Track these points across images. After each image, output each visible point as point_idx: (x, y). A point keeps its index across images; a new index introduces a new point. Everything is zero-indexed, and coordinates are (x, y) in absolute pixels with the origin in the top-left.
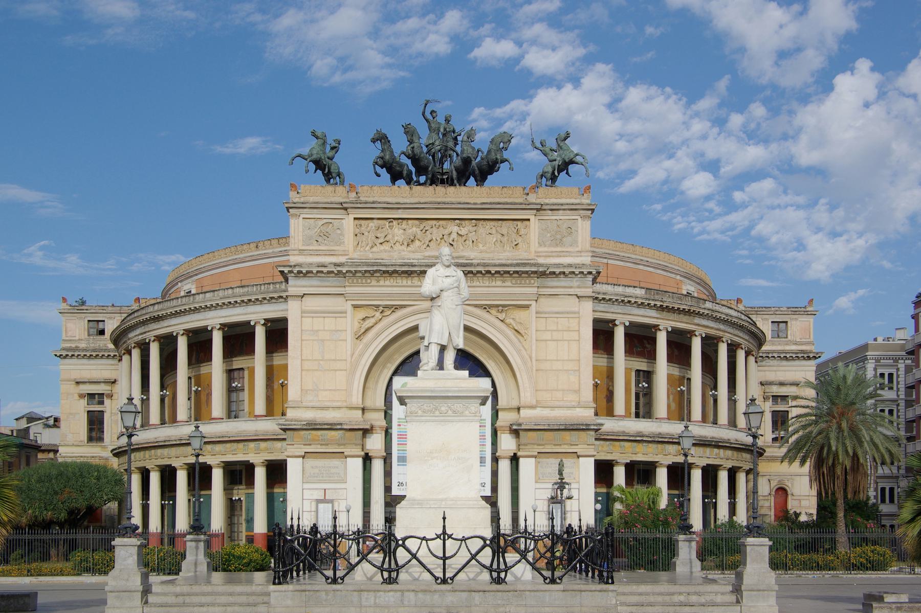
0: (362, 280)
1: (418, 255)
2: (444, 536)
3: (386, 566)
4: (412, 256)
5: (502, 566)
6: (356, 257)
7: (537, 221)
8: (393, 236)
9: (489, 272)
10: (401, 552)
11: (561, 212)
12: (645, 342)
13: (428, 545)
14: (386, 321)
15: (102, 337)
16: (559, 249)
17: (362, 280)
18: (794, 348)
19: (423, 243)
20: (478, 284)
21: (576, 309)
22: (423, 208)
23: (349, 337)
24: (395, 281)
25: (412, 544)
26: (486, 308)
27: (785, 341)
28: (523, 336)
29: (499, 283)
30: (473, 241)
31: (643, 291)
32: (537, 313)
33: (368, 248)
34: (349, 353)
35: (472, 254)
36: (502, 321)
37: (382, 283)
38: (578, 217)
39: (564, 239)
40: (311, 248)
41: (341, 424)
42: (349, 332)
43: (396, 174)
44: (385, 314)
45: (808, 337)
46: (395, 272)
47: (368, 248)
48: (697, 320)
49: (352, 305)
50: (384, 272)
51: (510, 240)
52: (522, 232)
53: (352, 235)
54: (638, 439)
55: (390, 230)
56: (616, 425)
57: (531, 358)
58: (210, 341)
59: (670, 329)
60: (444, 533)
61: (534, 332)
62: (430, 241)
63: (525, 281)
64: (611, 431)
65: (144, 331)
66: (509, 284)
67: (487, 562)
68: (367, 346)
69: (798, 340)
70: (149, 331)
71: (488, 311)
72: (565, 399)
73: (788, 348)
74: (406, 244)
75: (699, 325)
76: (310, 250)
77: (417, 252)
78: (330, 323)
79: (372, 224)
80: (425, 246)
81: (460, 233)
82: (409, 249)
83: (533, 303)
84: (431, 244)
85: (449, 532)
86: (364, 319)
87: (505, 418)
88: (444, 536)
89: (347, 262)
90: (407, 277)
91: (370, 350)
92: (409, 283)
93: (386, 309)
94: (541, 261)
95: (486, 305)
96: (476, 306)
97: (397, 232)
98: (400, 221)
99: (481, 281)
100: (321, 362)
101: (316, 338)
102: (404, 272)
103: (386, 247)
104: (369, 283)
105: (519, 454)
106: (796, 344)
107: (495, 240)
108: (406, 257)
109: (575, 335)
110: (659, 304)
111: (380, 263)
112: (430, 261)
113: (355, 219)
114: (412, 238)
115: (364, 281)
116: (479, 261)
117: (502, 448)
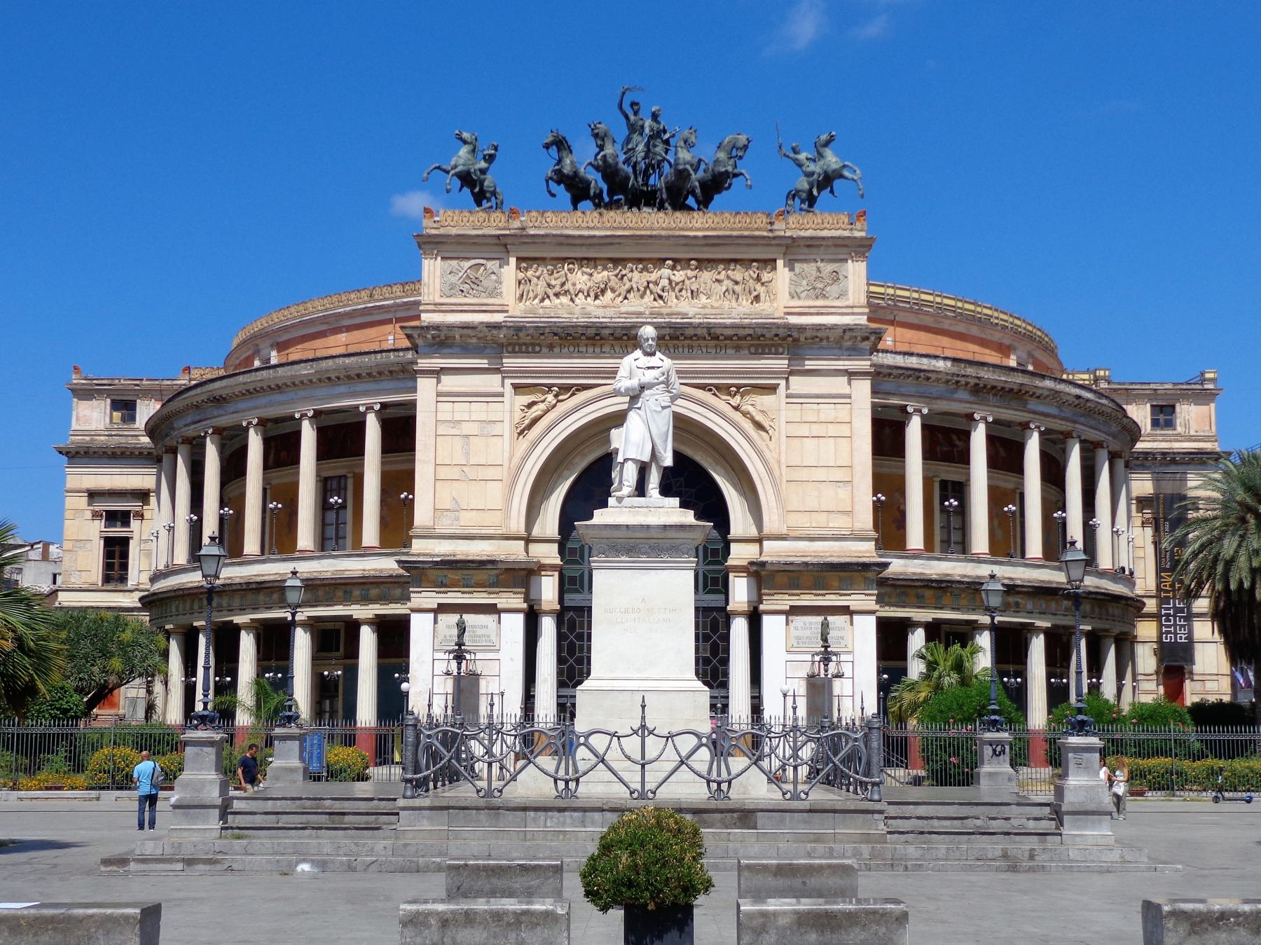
0: (527, 348)
1: (610, 312)
2: (643, 730)
3: (561, 773)
4: (600, 312)
5: (724, 775)
6: (519, 314)
8: (574, 285)
9: (717, 338)
10: (582, 752)
11: (822, 248)
12: (954, 437)
13: (620, 745)
14: (562, 408)
15: (132, 426)
16: (820, 303)
17: (527, 348)
19: (617, 293)
21: (846, 390)
22: (620, 243)
23: (506, 429)
24: (576, 349)
25: (599, 742)
27: (1173, 435)
28: (767, 432)
29: (730, 351)
30: (692, 292)
31: (949, 364)
32: (787, 397)
33: (537, 301)
34: (507, 455)
35: (691, 311)
37: (557, 350)
39: (828, 289)
40: (453, 300)
42: (507, 425)
43: (578, 191)
44: (561, 397)
45: (1207, 428)
47: (537, 301)
48: (1033, 406)
51: (747, 290)
53: (513, 283)
54: (941, 589)
55: (569, 275)
57: (779, 462)
58: (297, 435)
59: (990, 419)
60: (643, 727)
61: (783, 425)
62: (629, 291)
63: (770, 350)
64: (901, 574)
65: (197, 418)
67: (703, 769)
69: (1192, 433)
70: (205, 420)
71: (714, 394)
72: (831, 525)
73: (1176, 445)
74: (592, 294)
75: (1034, 412)
76: (452, 304)
77: (610, 307)
78: (479, 410)
80: (621, 299)
81: (672, 278)
82: (597, 302)
83: (783, 383)
84: (631, 296)
85: (650, 726)
86: (530, 405)
87: (740, 554)
88: (643, 730)
89: (504, 322)
90: (594, 345)
92: (598, 350)
93: (562, 392)
94: (794, 320)
97: (580, 278)
98: (586, 262)
99: (704, 350)
100: (465, 468)
101: (457, 432)
103: (565, 300)
104: (538, 352)
105: (762, 607)
107: (724, 289)
108: (593, 314)
109: (845, 430)
110: (973, 381)
111: (555, 322)
112: (628, 320)
114: (602, 286)
115: (530, 349)
116: (701, 321)
117: (737, 599)
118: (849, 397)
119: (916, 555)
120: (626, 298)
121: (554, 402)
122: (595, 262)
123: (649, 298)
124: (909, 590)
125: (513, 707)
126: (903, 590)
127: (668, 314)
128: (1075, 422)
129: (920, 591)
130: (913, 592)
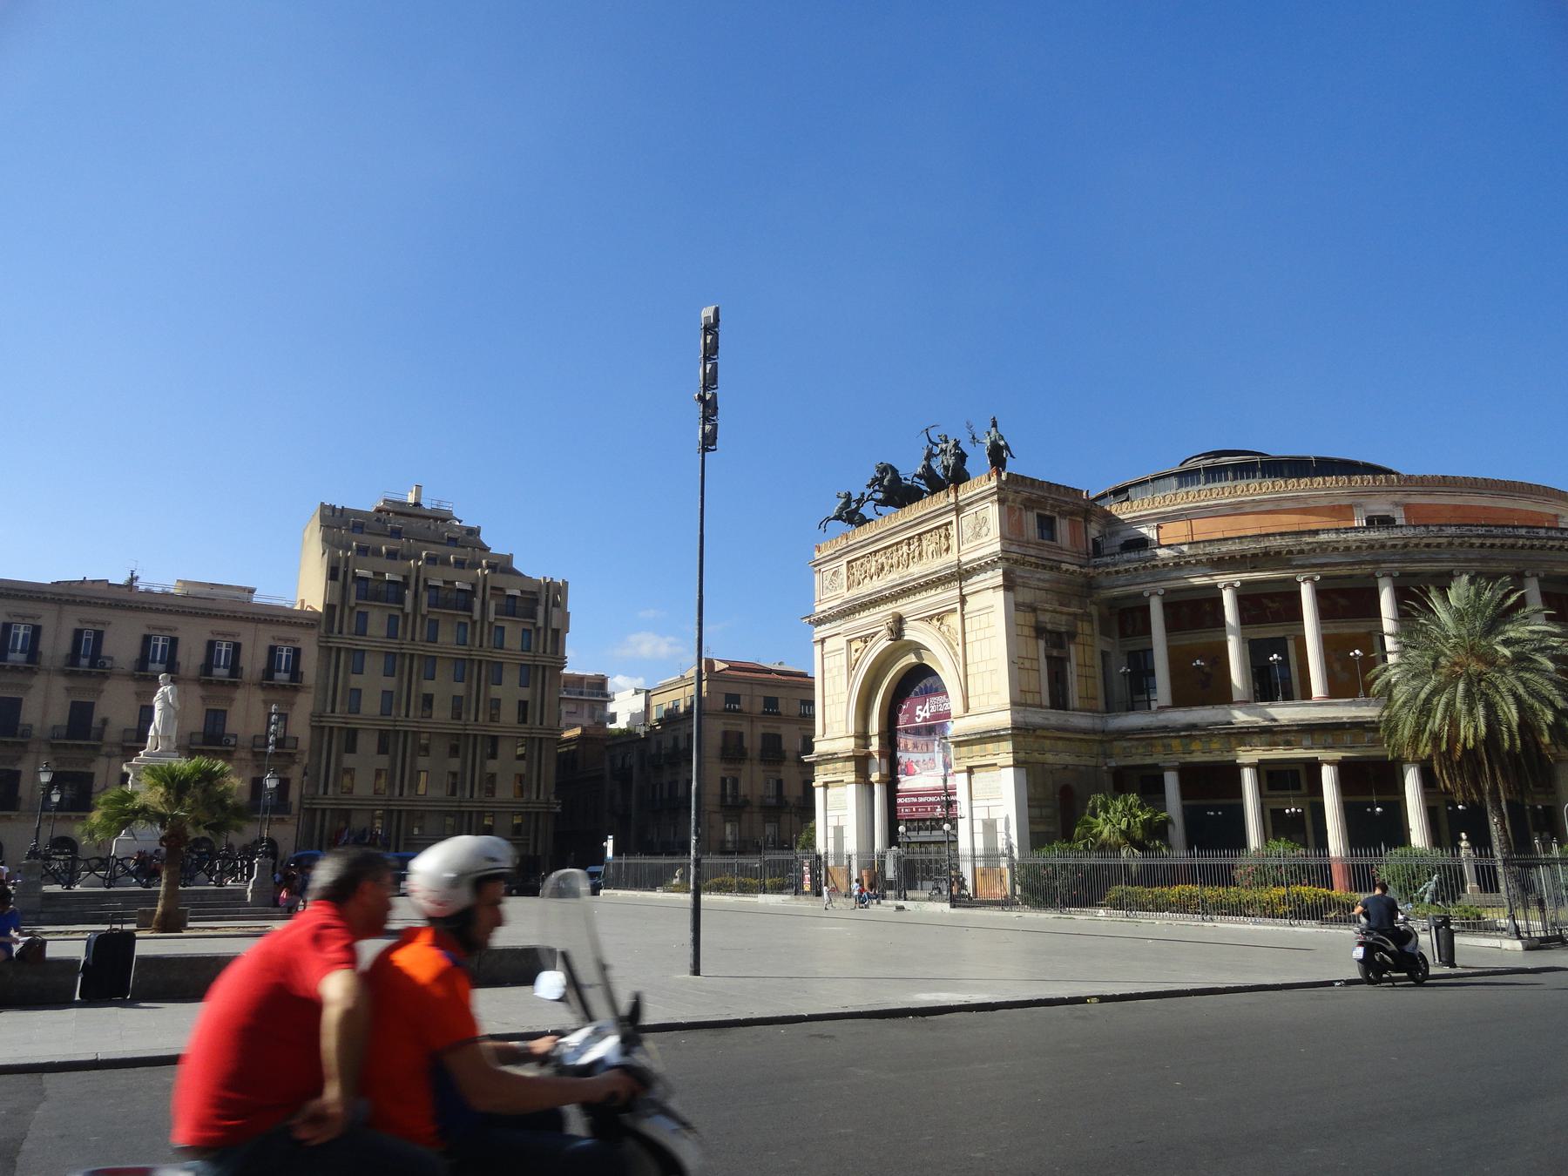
12: (1265, 601)
20: (919, 598)
29: (933, 592)
38: (989, 504)
41: (836, 753)
49: (848, 641)
56: (1154, 719)
66: (939, 590)
75: (1303, 567)
79: (859, 562)
83: (958, 605)
86: (856, 651)
95: (927, 617)
110: (1204, 558)
113: (849, 562)
114: (880, 567)
118: (992, 606)
124: (1154, 741)
125: (968, 846)
128: (1377, 562)
129: (1165, 741)
130: (1160, 742)
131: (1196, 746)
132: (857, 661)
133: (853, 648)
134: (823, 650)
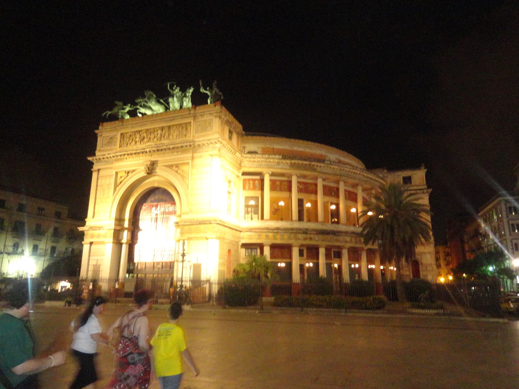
7: (195, 122)
18: (415, 188)
26: (170, 166)
36: (177, 172)
37: (128, 160)
46: (132, 154)
50: (128, 155)
52: (189, 128)
55: (134, 137)
66: (180, 153)
68: (119, 190)
69: (417, 184)
74: (140, 141)
82: (141, 143)
83: (190, 161)
86: (121, 177)
91: (120, 191)
92: (139, 158)
96: (166, 166)
102: (135, 154)
106: (416, 186)
107: (176, 134)
115: (121, 160)
119: (267, 220)
120: (149, 141)
121: (126, 176)
122: (142, 132)
123: (155, 139)
126: (260, 233)
127: (159, 144)
129: (267, 234)
131: (278, 236)
132: (121, 183)
133: (119, 176)
134: (98, 174)
